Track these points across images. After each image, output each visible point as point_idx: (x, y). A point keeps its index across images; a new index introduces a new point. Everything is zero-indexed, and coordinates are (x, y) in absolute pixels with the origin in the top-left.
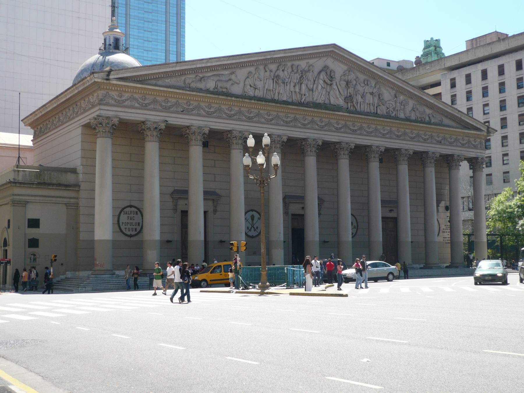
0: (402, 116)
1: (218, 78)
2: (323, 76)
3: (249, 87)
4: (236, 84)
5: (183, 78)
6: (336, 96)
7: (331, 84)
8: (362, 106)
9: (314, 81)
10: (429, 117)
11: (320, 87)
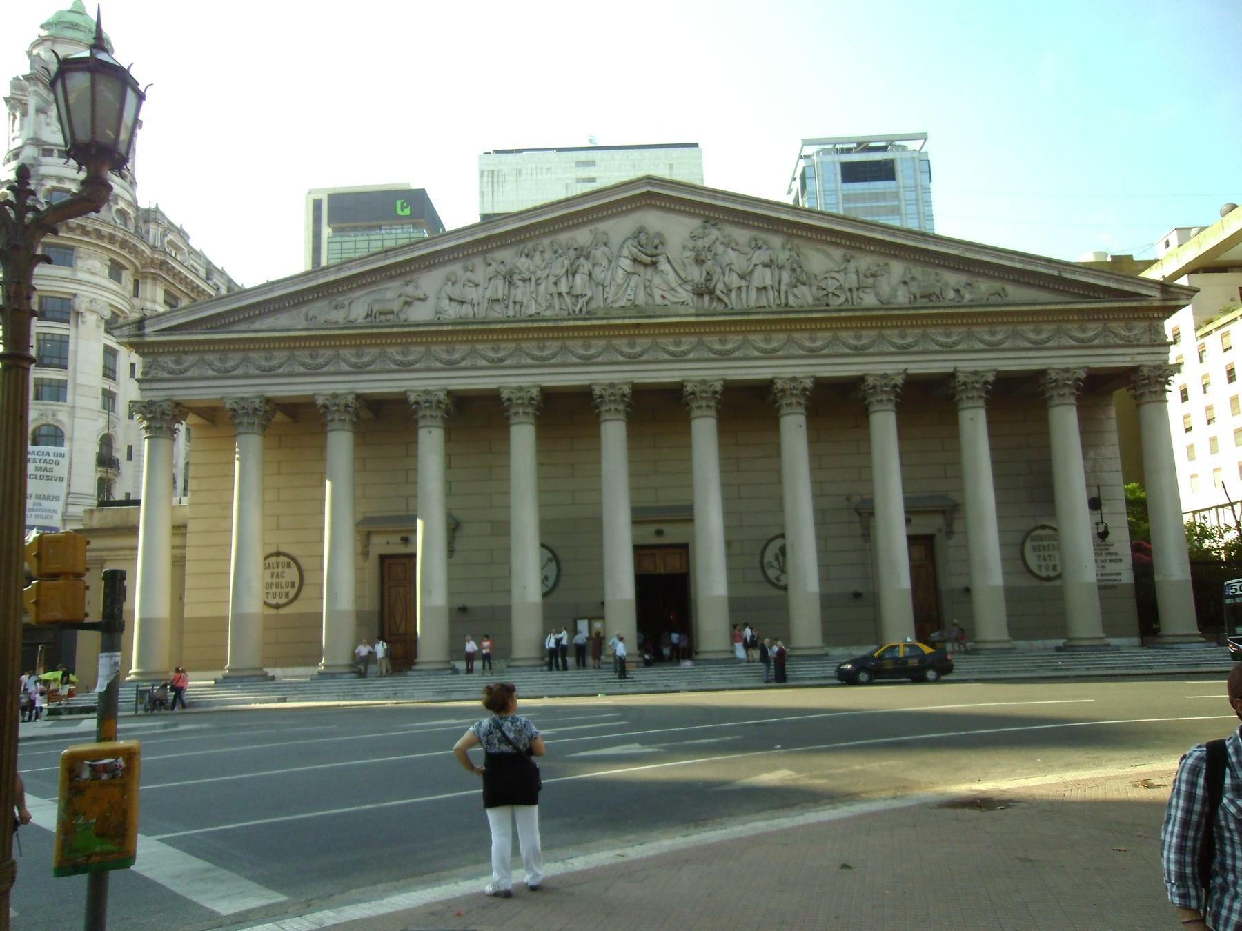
0: (869, 300)
1: (376, 296)
2: (630, 249)
3: (447, 301)
4: (418, 304)
5: (304, 310)
6: (668, 284)
7: (654, 264)
8: (744, 295)
9: (610, 262)
10: (957, 291)
11: (620, 273)
